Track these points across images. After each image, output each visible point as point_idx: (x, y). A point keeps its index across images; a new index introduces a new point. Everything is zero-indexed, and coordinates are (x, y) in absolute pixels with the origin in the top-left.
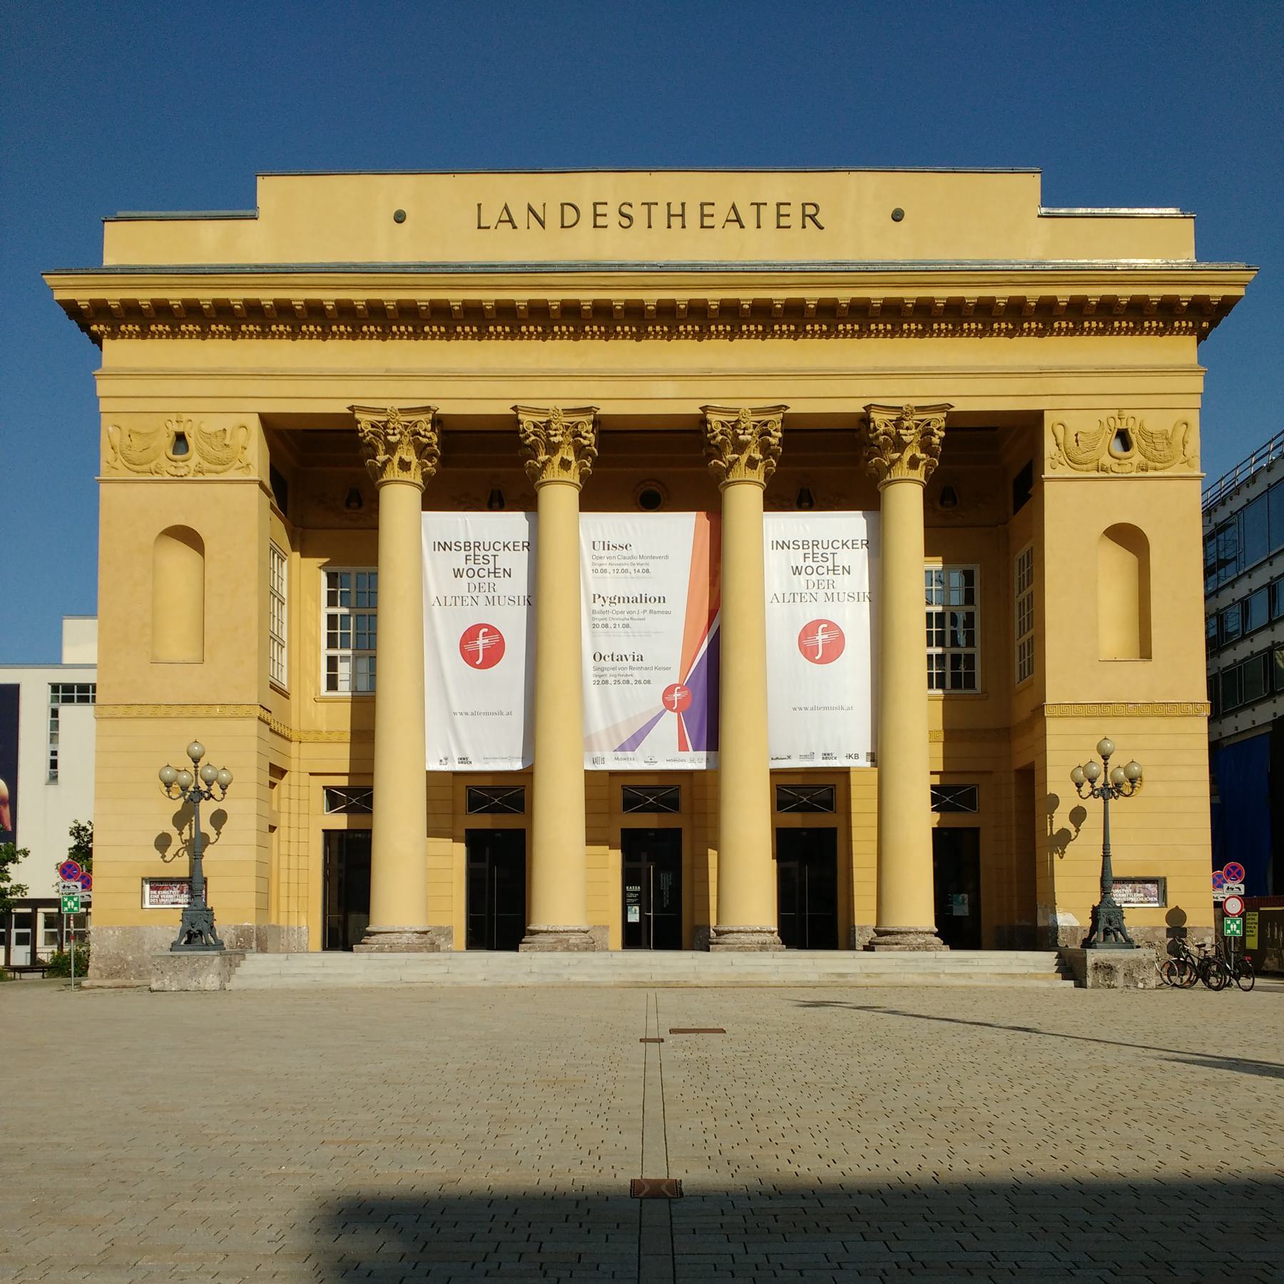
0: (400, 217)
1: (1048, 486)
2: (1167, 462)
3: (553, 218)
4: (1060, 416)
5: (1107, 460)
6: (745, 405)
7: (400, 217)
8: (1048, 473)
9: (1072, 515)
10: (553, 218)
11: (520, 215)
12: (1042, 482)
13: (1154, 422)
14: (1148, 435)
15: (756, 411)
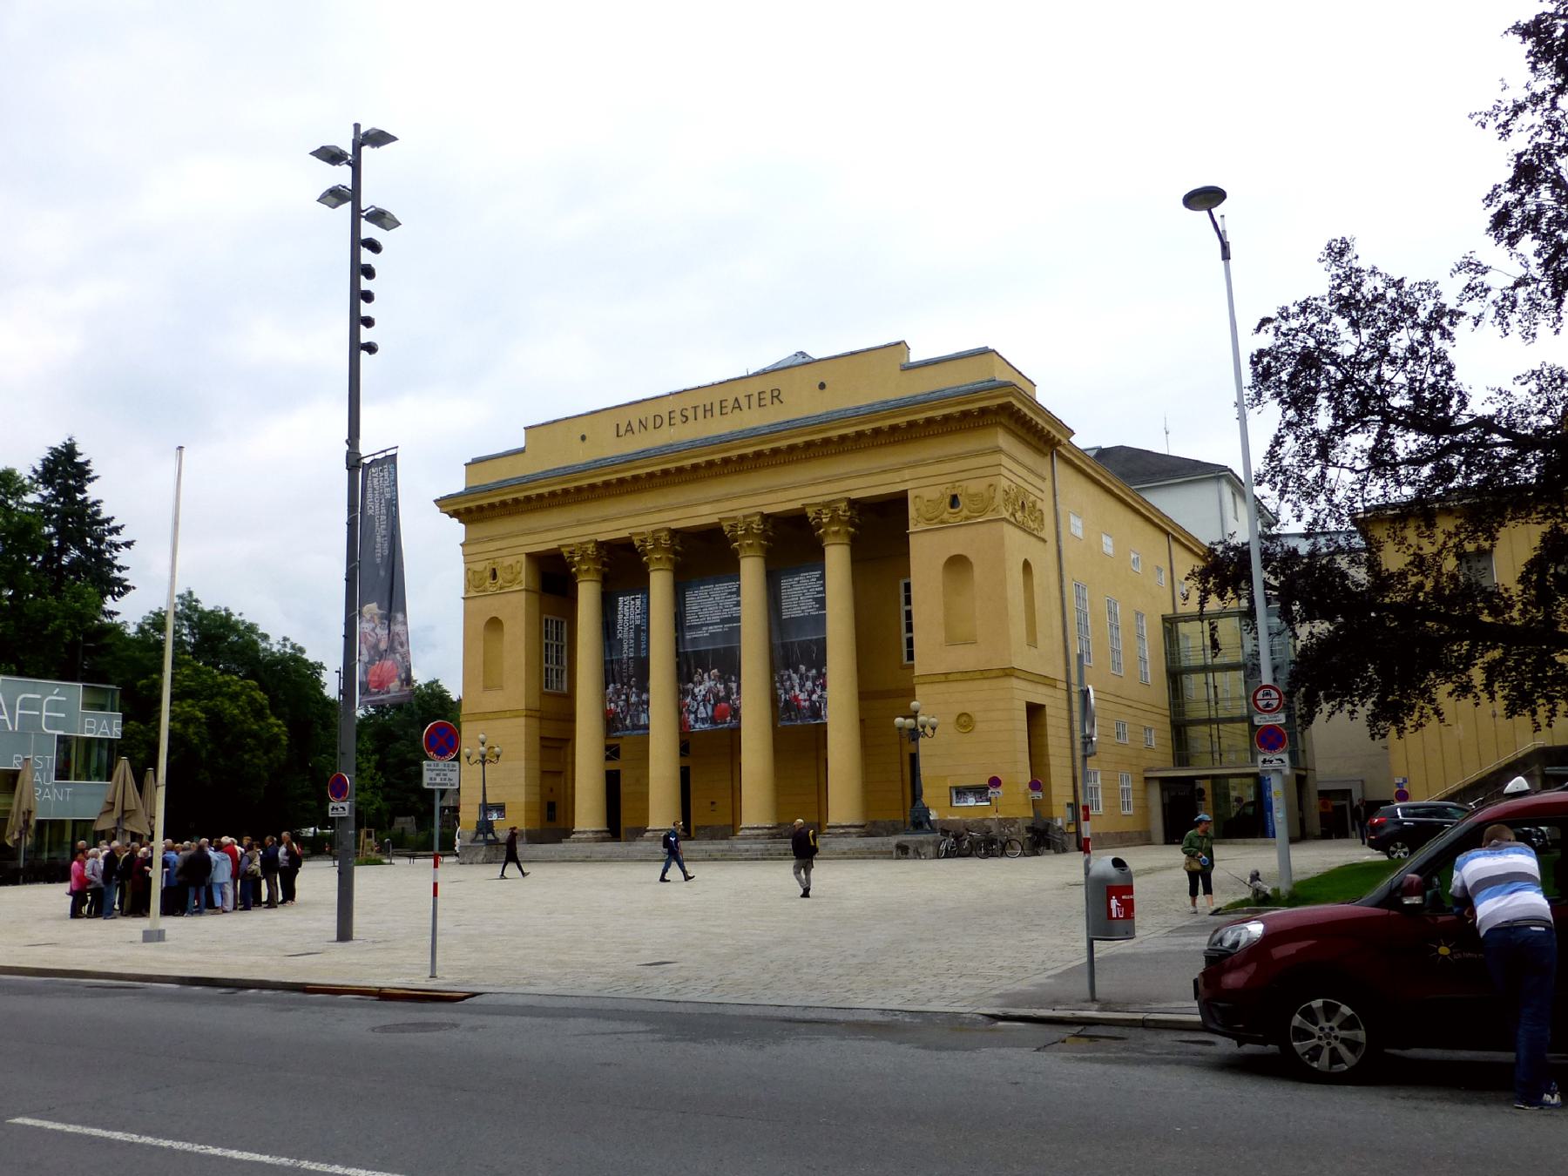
0: (583, 438)
1: (913, 541)
2: (983, 511)
3: (650, 425)
4: (916, 492)
5: (945, 516)
6: (739, 514)
7: (583, 438)
8: (912, 529)
9: (926, 552)
10: (650, 425)
11: (635, 426)
12: (907, 536)
13: (974, 487)
14: (972, 497)
15: (745, 517)
